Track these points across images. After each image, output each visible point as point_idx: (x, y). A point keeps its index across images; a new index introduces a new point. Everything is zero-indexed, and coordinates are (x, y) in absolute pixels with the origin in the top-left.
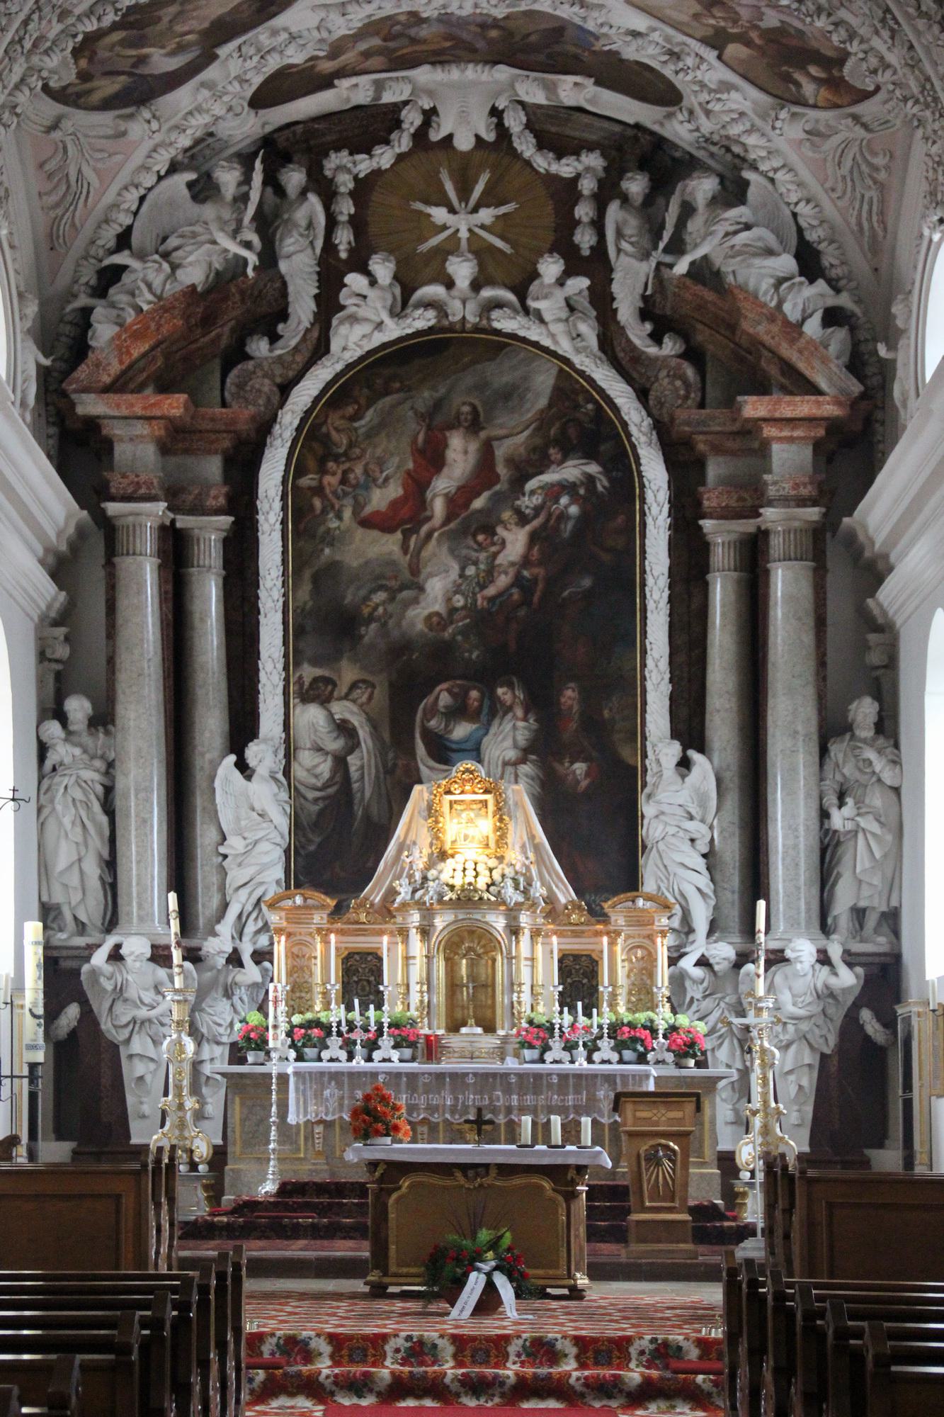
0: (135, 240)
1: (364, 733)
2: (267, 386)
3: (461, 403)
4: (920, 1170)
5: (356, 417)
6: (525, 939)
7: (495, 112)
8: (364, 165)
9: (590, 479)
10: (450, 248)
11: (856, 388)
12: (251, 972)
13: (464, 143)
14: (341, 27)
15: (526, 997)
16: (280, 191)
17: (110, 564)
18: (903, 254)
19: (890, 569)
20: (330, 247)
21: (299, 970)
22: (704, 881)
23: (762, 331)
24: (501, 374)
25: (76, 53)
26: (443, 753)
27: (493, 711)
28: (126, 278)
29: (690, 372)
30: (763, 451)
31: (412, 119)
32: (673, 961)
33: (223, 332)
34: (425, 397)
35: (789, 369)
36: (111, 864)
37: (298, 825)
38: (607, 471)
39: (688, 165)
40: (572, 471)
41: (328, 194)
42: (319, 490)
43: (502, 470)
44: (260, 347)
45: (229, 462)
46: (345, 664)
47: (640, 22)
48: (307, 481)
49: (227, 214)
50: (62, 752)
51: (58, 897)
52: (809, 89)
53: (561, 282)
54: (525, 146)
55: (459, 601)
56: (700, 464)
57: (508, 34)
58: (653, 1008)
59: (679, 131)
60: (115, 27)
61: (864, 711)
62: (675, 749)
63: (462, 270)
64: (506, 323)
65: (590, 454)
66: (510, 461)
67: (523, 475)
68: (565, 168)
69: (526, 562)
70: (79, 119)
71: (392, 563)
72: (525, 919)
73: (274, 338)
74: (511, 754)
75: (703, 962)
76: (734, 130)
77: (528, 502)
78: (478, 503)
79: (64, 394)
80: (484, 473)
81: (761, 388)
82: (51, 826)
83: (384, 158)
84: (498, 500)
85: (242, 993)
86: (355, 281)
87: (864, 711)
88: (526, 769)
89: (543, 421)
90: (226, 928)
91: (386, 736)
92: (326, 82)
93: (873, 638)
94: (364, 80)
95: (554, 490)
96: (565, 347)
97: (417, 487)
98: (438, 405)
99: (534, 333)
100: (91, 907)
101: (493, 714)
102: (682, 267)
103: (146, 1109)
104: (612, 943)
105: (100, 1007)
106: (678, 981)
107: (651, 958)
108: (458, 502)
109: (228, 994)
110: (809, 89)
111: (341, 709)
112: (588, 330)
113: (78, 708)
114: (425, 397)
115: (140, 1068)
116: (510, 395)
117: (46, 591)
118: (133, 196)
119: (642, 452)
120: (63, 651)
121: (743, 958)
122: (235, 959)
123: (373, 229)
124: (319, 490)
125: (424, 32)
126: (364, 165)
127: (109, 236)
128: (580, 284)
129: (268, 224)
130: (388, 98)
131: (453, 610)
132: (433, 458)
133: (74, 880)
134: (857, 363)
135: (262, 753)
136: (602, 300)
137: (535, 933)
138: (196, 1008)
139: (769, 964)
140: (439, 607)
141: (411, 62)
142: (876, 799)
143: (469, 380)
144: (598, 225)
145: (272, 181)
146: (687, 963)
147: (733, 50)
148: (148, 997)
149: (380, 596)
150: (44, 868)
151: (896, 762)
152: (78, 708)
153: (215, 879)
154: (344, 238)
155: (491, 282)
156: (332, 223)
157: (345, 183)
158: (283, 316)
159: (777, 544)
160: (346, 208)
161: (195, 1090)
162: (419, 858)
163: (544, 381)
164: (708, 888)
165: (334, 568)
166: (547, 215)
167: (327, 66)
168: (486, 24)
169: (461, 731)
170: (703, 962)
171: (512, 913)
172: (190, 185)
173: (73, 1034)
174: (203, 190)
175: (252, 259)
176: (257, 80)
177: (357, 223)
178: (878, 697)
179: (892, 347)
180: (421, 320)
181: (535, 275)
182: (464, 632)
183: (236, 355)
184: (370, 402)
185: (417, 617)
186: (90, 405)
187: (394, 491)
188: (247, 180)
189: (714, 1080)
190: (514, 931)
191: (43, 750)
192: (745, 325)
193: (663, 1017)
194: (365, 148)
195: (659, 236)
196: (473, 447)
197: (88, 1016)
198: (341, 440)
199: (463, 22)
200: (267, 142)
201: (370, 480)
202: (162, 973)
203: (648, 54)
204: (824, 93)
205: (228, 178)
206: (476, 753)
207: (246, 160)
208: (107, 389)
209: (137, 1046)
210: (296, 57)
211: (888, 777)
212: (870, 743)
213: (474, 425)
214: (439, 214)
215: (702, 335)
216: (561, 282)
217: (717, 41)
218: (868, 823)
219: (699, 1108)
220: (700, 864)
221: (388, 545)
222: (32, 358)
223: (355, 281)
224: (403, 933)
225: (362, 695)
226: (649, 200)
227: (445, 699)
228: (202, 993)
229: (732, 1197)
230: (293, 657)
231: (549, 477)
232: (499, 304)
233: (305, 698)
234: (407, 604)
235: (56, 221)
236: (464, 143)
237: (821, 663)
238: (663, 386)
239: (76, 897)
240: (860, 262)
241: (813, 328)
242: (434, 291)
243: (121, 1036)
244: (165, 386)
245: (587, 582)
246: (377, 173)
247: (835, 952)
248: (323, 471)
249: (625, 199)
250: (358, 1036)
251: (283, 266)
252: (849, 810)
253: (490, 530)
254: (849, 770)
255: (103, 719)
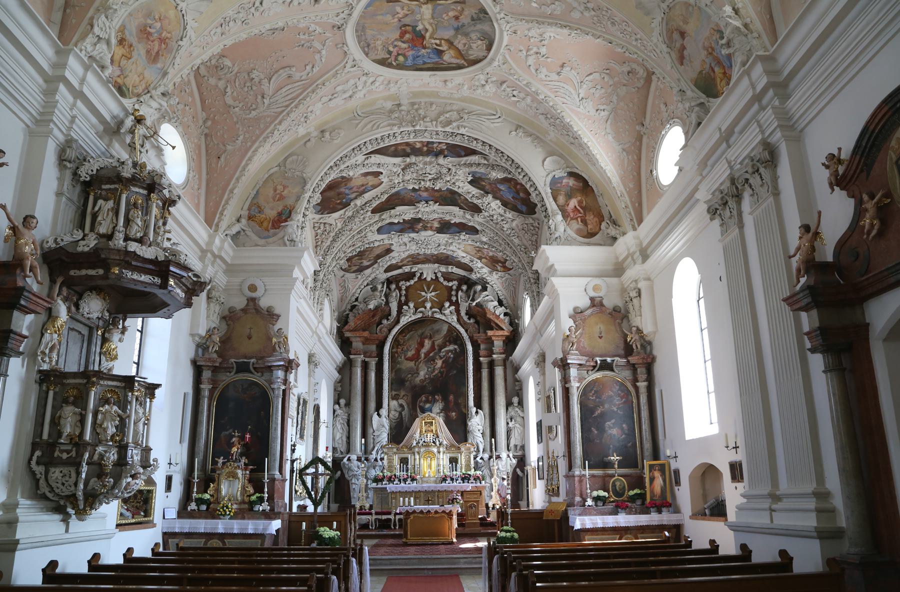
0: (359, 300)
1: (406, 407)
2: (386, 330)
3: (428, 333)
4: (531, 508)
5: (405, 336)
6: (441, 454)
7: (435, 273)
8: (408, 284)
9: (455, 349)
10: (425, 301)
11: (511, 329)
12: (380, 463)
13: (429, 279)
14: (404, 256)
15: (442, 468)
16: (390, 289)
17: (351, 369)
18: (520, 302)
19: (520, 368)
20: (400, 300)
21: (390, 461)
22: (481, 439)
23: (491, 317)
24: (436, 326)
25: (347, 260)
26: (423, 411)
27: (434, 401)
28: (357, 307)
29: (476, 326)
30: (492, 343)
31: (418, 275)
32: (475, 458)
33: (377, 318)
34: (420, 332)
35: (497, 325)
36: (348, 438)
37: (391, 428)
38: (459, 347)
39: (475, 283)
40: (451, 347)
41: (400, 289)
42: (397, 352)
43: (436, 347)
44: (385, 322)
45: (377, 346)
46: (402, 391)
47: (464, 255)
48: (394, 350)
49: (378, 294)
50: (339, 412)
51: (337, 446)
52: (499, 268)
53: (449, 307)
54: (441, 280)
55: (427, 376)
56: (479, 345)
57: (438, 257)
58: (470, 470)
59: (474, 277)
60: (356, 256)
61: (515, 400)
62: (474, 410)
63: (428, 305)
64: (438, 316)
65: (456, 344)
66: (438, 346)
67: (441, 347)
68: (450, 284)
69: (442, 367)
70: (348, 275)
71: (412, 368)
72: (441, 449)
73: (388, 320)
74: (439, 411)
75: (482, 458)
76: (484, 276)
77: (442, 354)
78: (431, 355)
79: (342, 332)
80: (433, 348)
81: (492, 329)
82: (336, 429)
83: (412, 282)
84: (436, 354)
85: (377, 468)
86: (405, 307)
87: (515, 400)
88: (441, 414)
89: (445, 336)
90: (374, 453)
91: (411, 407)
92: (400, 267)
93: (517, 383)
94: (408, 267)
95: (448, 352)
96: (450, 321)
97: (418, 351)
98: (423, 334)
99: (443, 318)
100: (344, 449)
101: (434, 402)
102: (474, 304)
103: (355, 496)
104: (461, 455)
105: (345, 471)
106: (476, 463)
107: (470, 457)
108: (427, 354)
109: (374, 468)
110: (499, 268)
111: (401, 401)
112: (455, 318)
113: (342, 402)
114: (420, 332)
115: (354, 486)
116: (438, 331)
117: (336, 375)
118: (359, 290)
119: (467, 343)
120: (340, 389)
121: (491, 457)
122: (376, 460)
123: (409, 297)
124: (397, 352)
125: (420, 257)
126: (408, 284)
127: (353, 299)
128: (453, 308)
129: (386, 296)
130: (413, 270)
131: (426, 378)
132: (421, 345)
133: (340, 442)
134: (511, 323)
135: (384, 412)
136: (458, 311)
137: (444, 452)
138: (367, 472)
139: (496, 459)
140: (422, 378)
141: (418, 263)
142: (519, 419)
143: (429, 328)
144: (457, 296)
145: (388, 287)
146: (478, 459)
147: (483, 260)
148: (356, 469)
149: (410, 376)
150: (334, 439)
151: (523, 411)
152: (342, 402)
153: (372, 441)
154: (403, 298)
155: (434, 308)
156: (401, 295)
157: (404, 288)
158: (390, 315)
159: (496, 363)
160: (404, 292)
161: (366, 491)
162: (417, 435)
163: (445, 328)
164: (482, 441)
165: (400, 369)
166: (446, 294)
167: (400, 264)
168: (433, 255)
169: (428, 406)
170: (482, 458)
171: (439, 448)
172: (371, 288)
173: (339, 478)
174: (374, 289)
175: (384, 303)
176: (386, 266)
177: (406, 296)
178: (518, 396)
179: (518, 320)
180: (419, 315)
181: (444, 306)
182: (428, 383)
183: (380, 323)
184: (409, 333)
185: (418, 380)
186: (347, 334)
187: (413, 352)
188: (383, 287)
189: (484, 487)
190: (439, 452)
191: (334, 411)
192: (488, 316)
193: (472, 472)
194: (408, 280)
195: (469, 298)
196: (430, 343)
197: (343, 474)
198: (402, 341)
199: (428, 255)
200: (388, 279)
201: (408, 350)
202: (359, 463)
203: (466, 261)
204: (502, 269)
205: (379, 287)
206: (431, 411)
207: (383, 283)
208: (351, 331)
209: (353, 481)
210: (394, 262)
211: (521, 415)
212: (517, 407)
213: (431, 338)
214: (423, 293)
215: (479, 318)
216: (449, 307)
217: (480, 258)
218: (517, 425)
219: (481, 494)
220: (481, 435)
221: (411, 364)
222: (335, 324)
223: (405, 307)
224: (414, 454)
225: (405, 398)
226: (467, 291)
227: (424, 399)
228: (368, 469)
229: (488, 514)
230: (391, 389)
231: (446, 349)
232: (436, 312)
233: (393, 399)
234: (415, 377)
235: (343, 296)
236: (429, 279)
237: (506, 389)
238: (471, 329)
239: (340, 446)
240: (511, 303)
241: (502, 316)
242: (422, 309)
243: (349, 479)
244: (364, 330)
245: (455, 372)
246: (410, 285)
247: (511, 455)
248: (398, 348)
249: (462, 290)
250: (402, 478)
251: (390, 305)
252: (513, 422)
253: (434, 361)
254: (513, 413)
255: (348, 404)
